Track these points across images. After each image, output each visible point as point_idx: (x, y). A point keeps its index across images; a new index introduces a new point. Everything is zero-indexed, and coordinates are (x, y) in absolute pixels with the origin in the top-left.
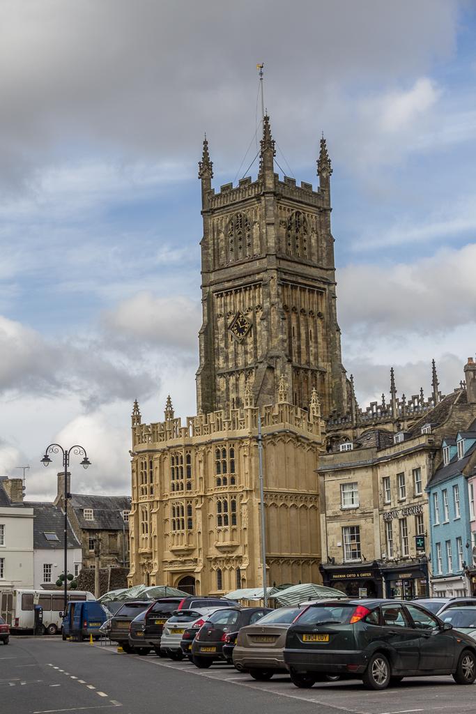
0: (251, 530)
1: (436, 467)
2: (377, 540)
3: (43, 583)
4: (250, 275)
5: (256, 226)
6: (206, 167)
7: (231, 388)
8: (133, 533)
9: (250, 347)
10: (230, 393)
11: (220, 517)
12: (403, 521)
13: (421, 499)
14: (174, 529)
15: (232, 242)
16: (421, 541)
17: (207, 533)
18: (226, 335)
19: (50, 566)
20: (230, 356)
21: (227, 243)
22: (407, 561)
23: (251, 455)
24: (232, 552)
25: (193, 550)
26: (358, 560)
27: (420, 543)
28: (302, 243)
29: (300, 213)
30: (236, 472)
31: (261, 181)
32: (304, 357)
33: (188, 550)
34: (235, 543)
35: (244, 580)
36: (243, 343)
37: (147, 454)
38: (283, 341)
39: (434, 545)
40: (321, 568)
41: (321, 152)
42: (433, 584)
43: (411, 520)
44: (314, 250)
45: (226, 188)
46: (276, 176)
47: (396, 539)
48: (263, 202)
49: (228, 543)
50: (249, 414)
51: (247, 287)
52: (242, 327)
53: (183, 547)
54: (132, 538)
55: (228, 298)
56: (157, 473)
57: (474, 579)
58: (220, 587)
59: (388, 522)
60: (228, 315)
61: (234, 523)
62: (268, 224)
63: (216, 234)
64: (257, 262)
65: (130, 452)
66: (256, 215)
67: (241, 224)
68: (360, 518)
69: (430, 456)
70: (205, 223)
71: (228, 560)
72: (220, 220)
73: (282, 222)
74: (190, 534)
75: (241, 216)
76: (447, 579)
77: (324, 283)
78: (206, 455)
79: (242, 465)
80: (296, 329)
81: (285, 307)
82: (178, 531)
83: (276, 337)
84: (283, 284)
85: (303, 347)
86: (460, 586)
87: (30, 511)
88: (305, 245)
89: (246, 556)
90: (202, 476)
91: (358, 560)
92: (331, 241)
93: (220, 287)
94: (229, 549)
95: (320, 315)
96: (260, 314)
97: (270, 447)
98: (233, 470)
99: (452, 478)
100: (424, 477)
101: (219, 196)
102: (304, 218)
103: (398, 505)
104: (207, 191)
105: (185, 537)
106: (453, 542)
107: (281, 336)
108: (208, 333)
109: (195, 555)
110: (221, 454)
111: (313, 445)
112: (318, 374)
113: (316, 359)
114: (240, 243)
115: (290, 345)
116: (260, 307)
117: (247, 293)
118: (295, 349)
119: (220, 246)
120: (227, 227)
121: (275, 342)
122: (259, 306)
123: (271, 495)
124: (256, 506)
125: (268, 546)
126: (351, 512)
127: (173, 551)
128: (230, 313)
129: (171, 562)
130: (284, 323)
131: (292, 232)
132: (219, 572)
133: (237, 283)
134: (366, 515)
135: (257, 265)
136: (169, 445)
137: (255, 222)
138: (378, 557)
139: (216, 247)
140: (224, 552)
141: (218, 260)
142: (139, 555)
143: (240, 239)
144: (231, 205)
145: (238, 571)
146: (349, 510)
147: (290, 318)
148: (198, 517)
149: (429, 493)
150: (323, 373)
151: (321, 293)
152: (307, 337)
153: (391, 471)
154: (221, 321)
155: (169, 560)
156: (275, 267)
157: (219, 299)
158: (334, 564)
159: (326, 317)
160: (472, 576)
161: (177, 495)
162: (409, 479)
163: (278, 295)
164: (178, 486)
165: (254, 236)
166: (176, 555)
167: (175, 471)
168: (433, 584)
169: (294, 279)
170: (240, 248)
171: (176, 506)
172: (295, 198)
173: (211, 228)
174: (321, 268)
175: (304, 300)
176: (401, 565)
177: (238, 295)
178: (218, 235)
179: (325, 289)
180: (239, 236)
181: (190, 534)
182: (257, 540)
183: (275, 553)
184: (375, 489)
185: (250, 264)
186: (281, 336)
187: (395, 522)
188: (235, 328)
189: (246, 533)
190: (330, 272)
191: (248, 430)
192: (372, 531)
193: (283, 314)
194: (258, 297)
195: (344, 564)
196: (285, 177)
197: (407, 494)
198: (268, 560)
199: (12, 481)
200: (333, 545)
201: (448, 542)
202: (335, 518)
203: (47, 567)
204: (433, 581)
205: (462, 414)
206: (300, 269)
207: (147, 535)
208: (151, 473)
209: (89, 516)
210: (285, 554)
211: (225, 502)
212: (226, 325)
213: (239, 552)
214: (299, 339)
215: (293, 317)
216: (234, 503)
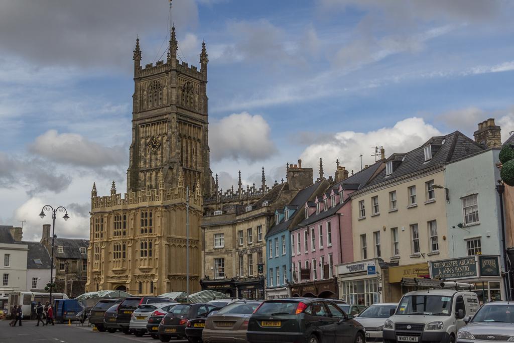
0: (160, 259)
1: (271, 225)
2: (234, 267)
3: (31, 289)
4: (161, 116)
5: (165, 88)
6: (137, 55)
7: (147, 179)
8: (90, 260)
9: (159, 156)
11: (142, 252)
12: (250, 256)
13: (261, 243)
14: (115, 258)
15: (151, 96)
16: (261, 268)
17: (135, 261)
18: (145, 149)
19: (36, 279)
20: (147, 161)
21: (148, 97)
22: (252, 278)
23: (162, 216)
24: (149, 272)
25: (125, 270)
26: (223, 278)
27: (260, 268)
28: (190, 100)
29: (190, 83)
30: (153, 226)
31: (169, 63)
32: (189, 163)
33: (122, 270)
34: (150, 267)
35: (155, 288)
36: (155, 154)
37: (100, 214)
38: (178, 153)
39: (269, 270)
40: (201, 282)
41: (202, 50)
42: (267, 292)
43: (255, 255)
44: (197, 104)
45: (149, 66)
46: (178, 61)
47: (245, 266)
48: (170, 75)
49: (146, 267)
50: (162, 192)
51: (158, 123)
52: (155, 145)
53: (119, 269)
54: (89, 263)
55: (148, 128)
56: (105, 226)
57: (293, 289)
58: (141, 293)
59: (241, 256)
60: (146, 138)
61: (150, 255)
62: (173, 87)
65: (90, 212)
66: (165, 82)
67: (157, 87)
68: (225, 253)
69: (268, 219)
70: (136, 85)
71: (146, 277)
72: (146, 84)
73: (180, 87)
74: (124, 261)
76: (276, 289)
77: (202, 123)
78: (135, 216)
79: (156, 222)
80: (185, 147)
81: (180, 135)
82: (117, 259)
83: (175, 151)
84: (179, 122)
85: (189, 158)
86: (285, 293)
87: (26, 247)
88: (192, 101)
89: (157, 274)
90: (132, 227)
91: (223, 278)
92: (206, 99)
93: (143, 121)
94: (147, 270)
95: (199, 140)
96: (166, 137)
97: (173, 212)
98: (151, 225)
99: (282, 231)
100: (264, 231)
101: (144, 70)
102: (192, 86)
103: (248, 247)
104: (137, 67)
105: (121, 263)
106: (281, 268)
107: (177, 151)
108: (135, 147)
109: (127, 273)
110: (144, 215)
111: (197, 212)
112: (197, 173)
113: (196, 165)
114: (156, 97)
115: (182, 156)
116: (166, 134)
117: (159, 125)
118: (184, 159)
119: (144, 98)
120: (148, 88)
121: (174, 154)
122: (165, 133)
123: (175, 240)
124: (164, 245)
125: (169, 268)
126: (220, 250)
127: (113, 271)
129: (112, 277)
130: (179, 143)
131: (185, 93)
132: (140, 283)
134: (228, 252)
135: (165, 110)
138: (234, 276)
139: (141, 99)
140: (144, 272)
141: (143, 106)
142: (93, 273)
144: (152, 75)
145: (152, 283)
146: (219, 249)
147: (182, 141)
148: (129, 251)
149: (267, 240)
150: (199, 173)
151: (200, 128)
152: (191, 152)
153: (244, 227)
154: (143, 141)
155: (111, 276)
156: (175, 112)
157: (142, 129)
158: (208, 280)
159: (202, 142)
160: (292, 288)
161: (117, 238)
162: (255, 232)
163: (176, 128)
164: (118, 233)
165: (164, 94)
166: (115, 273)
167: (117, 224)
168: (267, 292)
169: (185, 119)
170: (156, 100)
172: (188, 74)
173: (139, 88)
174: (201, 114)
175: (191, 132)
176: (248, 281)
177: (153, 127)
178: (143, 92)
179: (202, 126)
181: (124, 261)
182: (164, 265)
183: (173, 273)
184: (234, 237)
185: (161, 109)
186: (177, 151)
187: (245, 256)
189: (157, 262)
190: (205, 117)
191: (161, 202)
192: (232, 261)
193: (179, 139)
194: (165, 128)
195: (214, 280)
196: (183, 62)
197: (253, 240)
198: (169, 277)
199: (16, 228)
200: (208, 269)
201: (277, 268)
202: (210, 253)
203: (35, 280)
204: (267, 290)
205: (286, 196)
206: (188, 113)
207: (98, 261)
208: (102, 225)
209: (61, 250)
210: (179, 274)
211: (146, 243)
213: (153, 272)
214: (187, 153)
215: (184, 140)
216: (151, 244)
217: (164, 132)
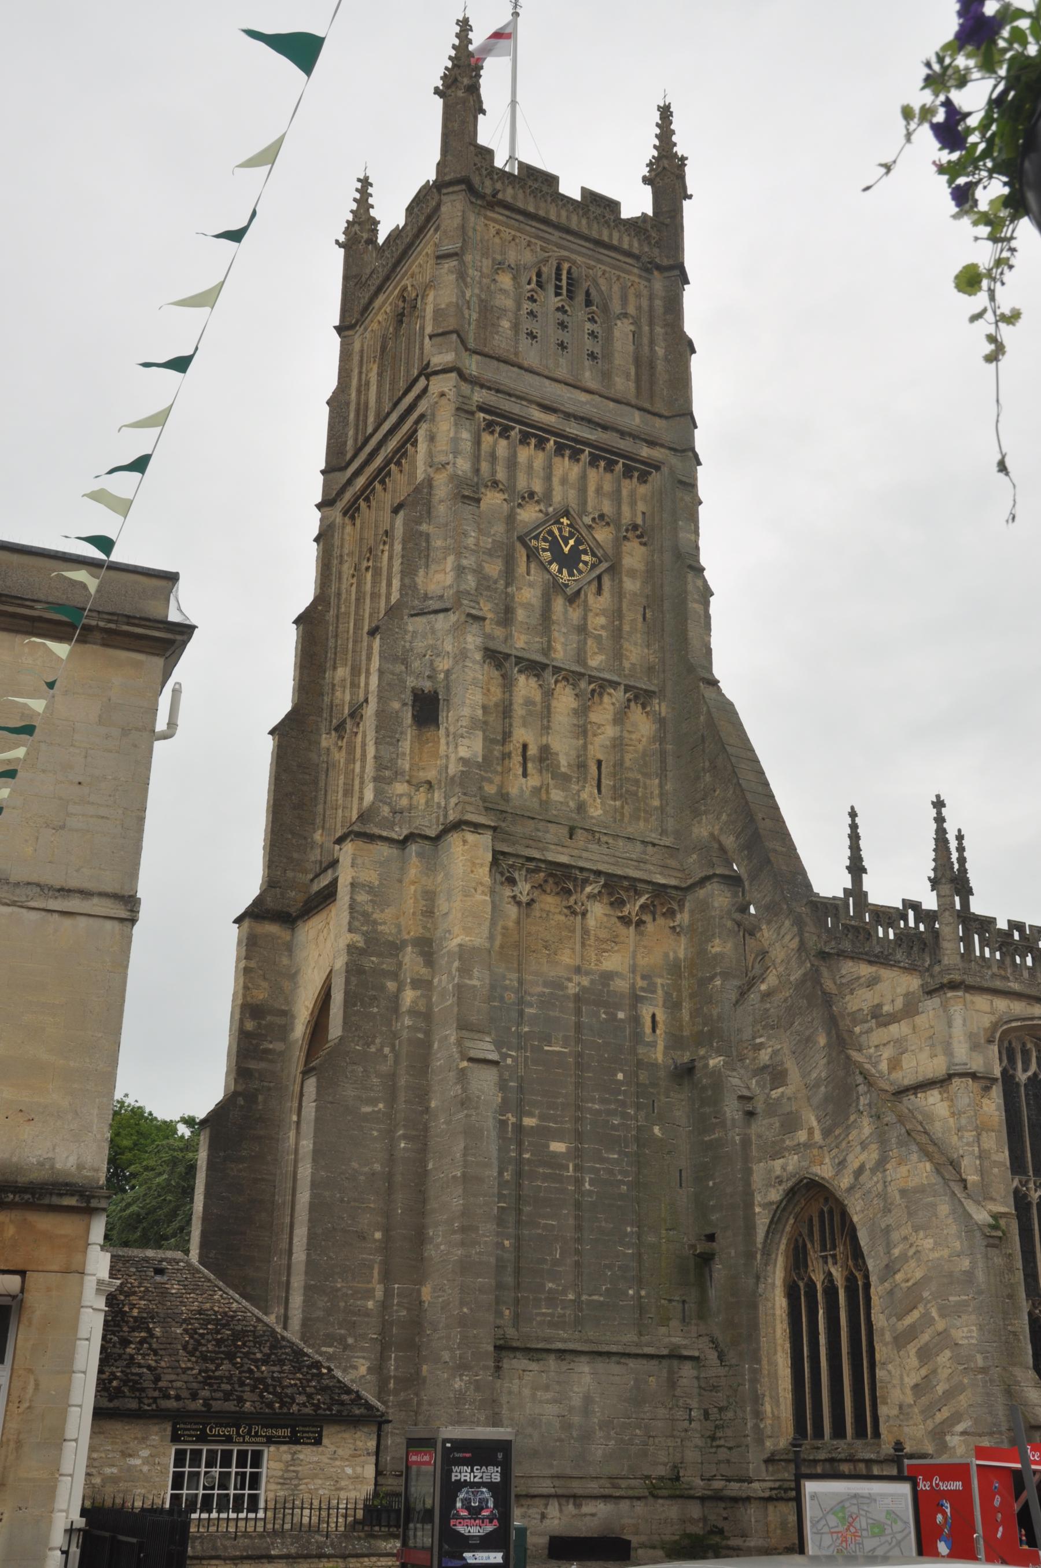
7: (519, 711)
10: (517, 722)
20: (521, 614)
64: (637, 414)
133: (573, 429)
137: (625, 315)
180: (559, 315)
185: (612, 404)
188: (546, 545)
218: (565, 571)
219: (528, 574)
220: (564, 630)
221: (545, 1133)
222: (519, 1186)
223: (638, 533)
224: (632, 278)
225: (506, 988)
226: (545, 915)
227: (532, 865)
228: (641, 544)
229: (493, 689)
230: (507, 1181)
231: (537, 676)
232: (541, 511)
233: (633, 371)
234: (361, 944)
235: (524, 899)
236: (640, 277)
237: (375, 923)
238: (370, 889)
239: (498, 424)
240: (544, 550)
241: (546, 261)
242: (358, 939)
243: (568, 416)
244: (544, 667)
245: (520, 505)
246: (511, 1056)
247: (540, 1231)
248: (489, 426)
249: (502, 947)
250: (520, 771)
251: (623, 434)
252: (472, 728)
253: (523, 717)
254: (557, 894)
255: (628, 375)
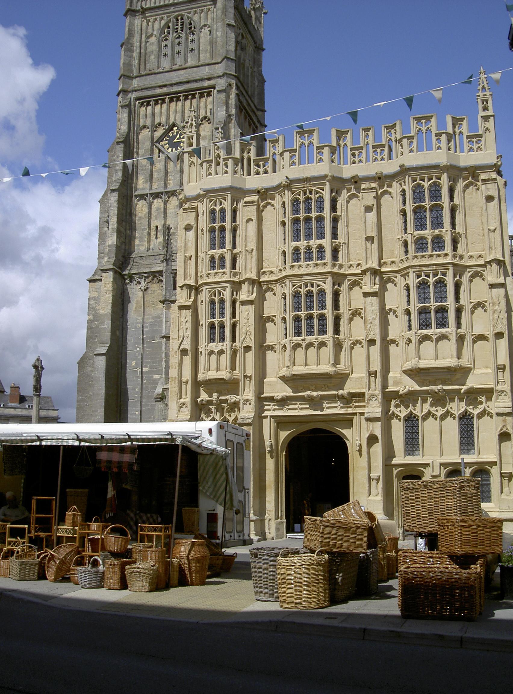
5: (206, 31)
7: (154, 213)
20: (155, 175)
21: (159, 47)
51: (189, 95)
60: (155, 127)
63: (144, 36)
64: (207, 67)
75: (182, 19)
92: (263, 81)
119: (148, 50)
122: (205, 118)
128: (160, 124)
133: (175, 89)
135: (205, 71)
136: (291, 177)
137: (205, 25)
143: (179, 44)
155: (279, 395)
157: (143, 109)
171: (303, 291)
178: (148, 37)
185: (195, 69)
207: (226, 345)
212: (152, 138)
217: (202, 114)
218: (174, 149)
219: (159, 157)
220: (173, 174)
221: (151, 373)
222: (141, 393)
223: (207, 119)
224: (208, 7)
225: (137, 323)
226: (153, 292)
227: (146, 275)
228: (209, 123)
229: (144, 209)
230: (137, 392)
231: (161, 198)
232: (164, 129)
233: (209, 48)
234: (92, 319)
235: (143, 288)
236: (211, 5)
237: (97, 310)
238: (95, 298)
239: (145, 102)
240: (165, 145)
241: (169, 21)
242: (91, 317)
243: (172, 85)
244: (162, 193)
245: (155, 131)
246: (139, 347)
247: (149, 407)
248: (142, 104)
249: (136, 308)
250: (155, 236)
251: (196, 81)
252: (112, 233)
253: (156, 216)
254: (158, 282)
255: (206, 51)
